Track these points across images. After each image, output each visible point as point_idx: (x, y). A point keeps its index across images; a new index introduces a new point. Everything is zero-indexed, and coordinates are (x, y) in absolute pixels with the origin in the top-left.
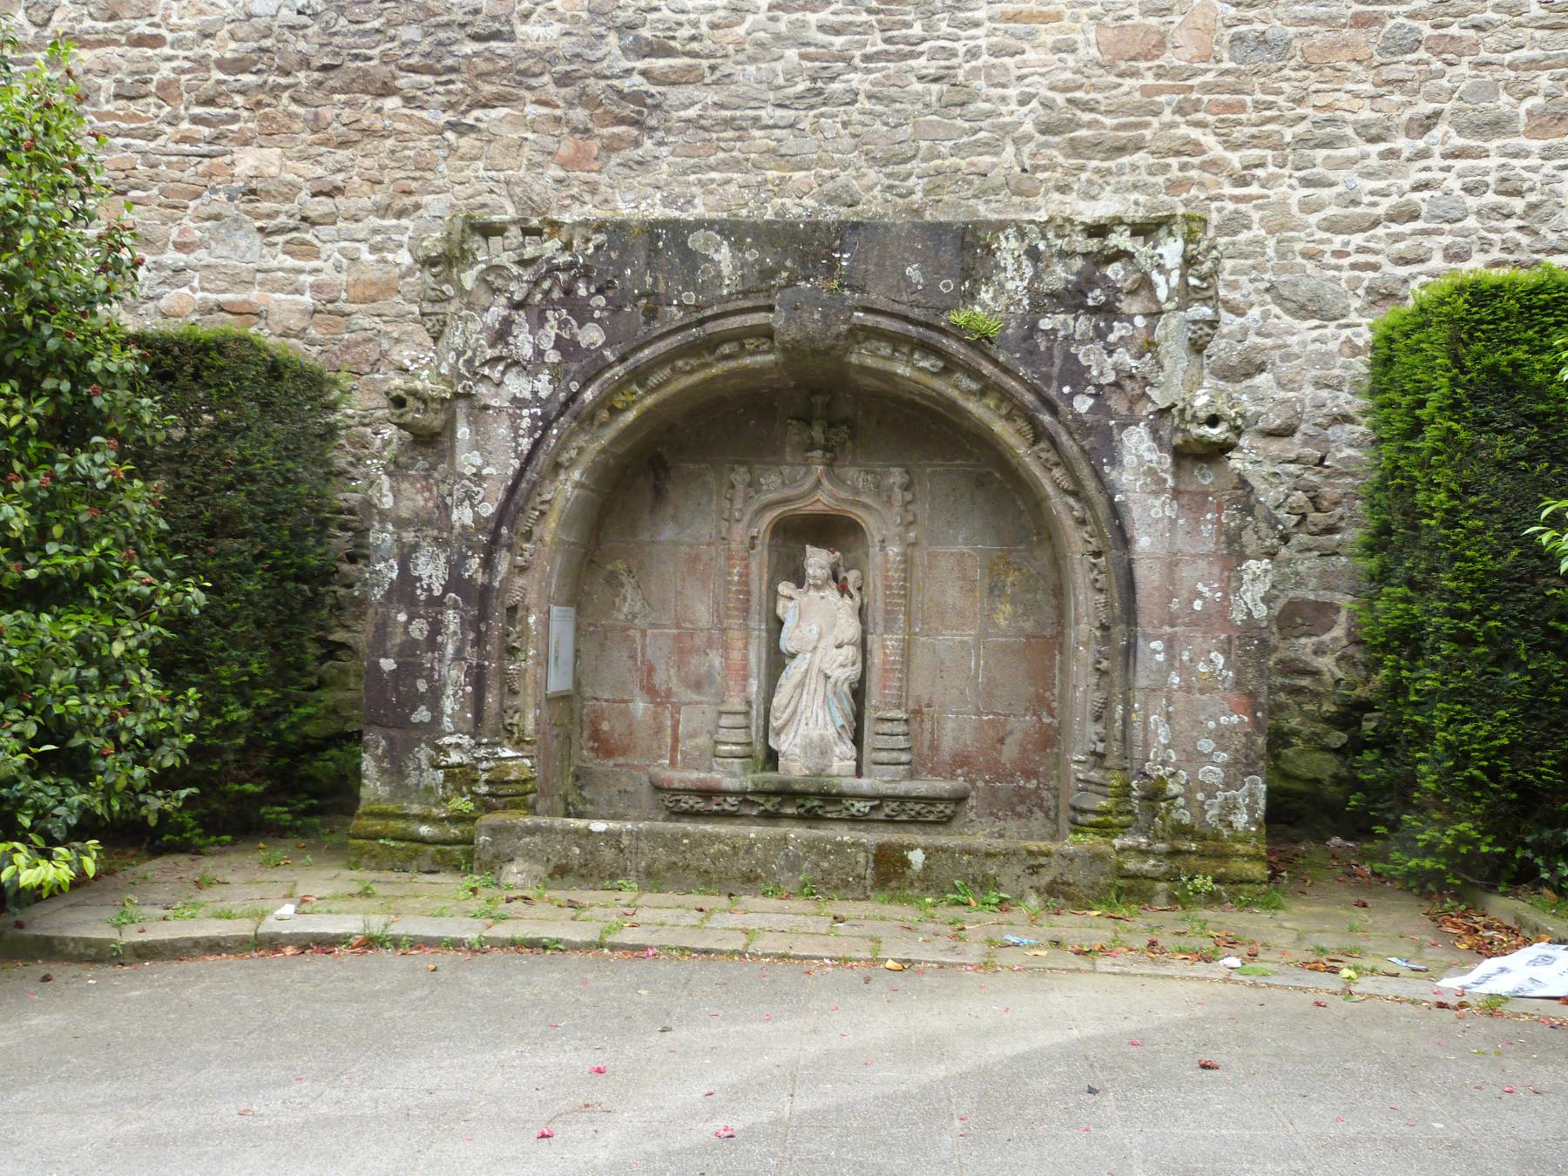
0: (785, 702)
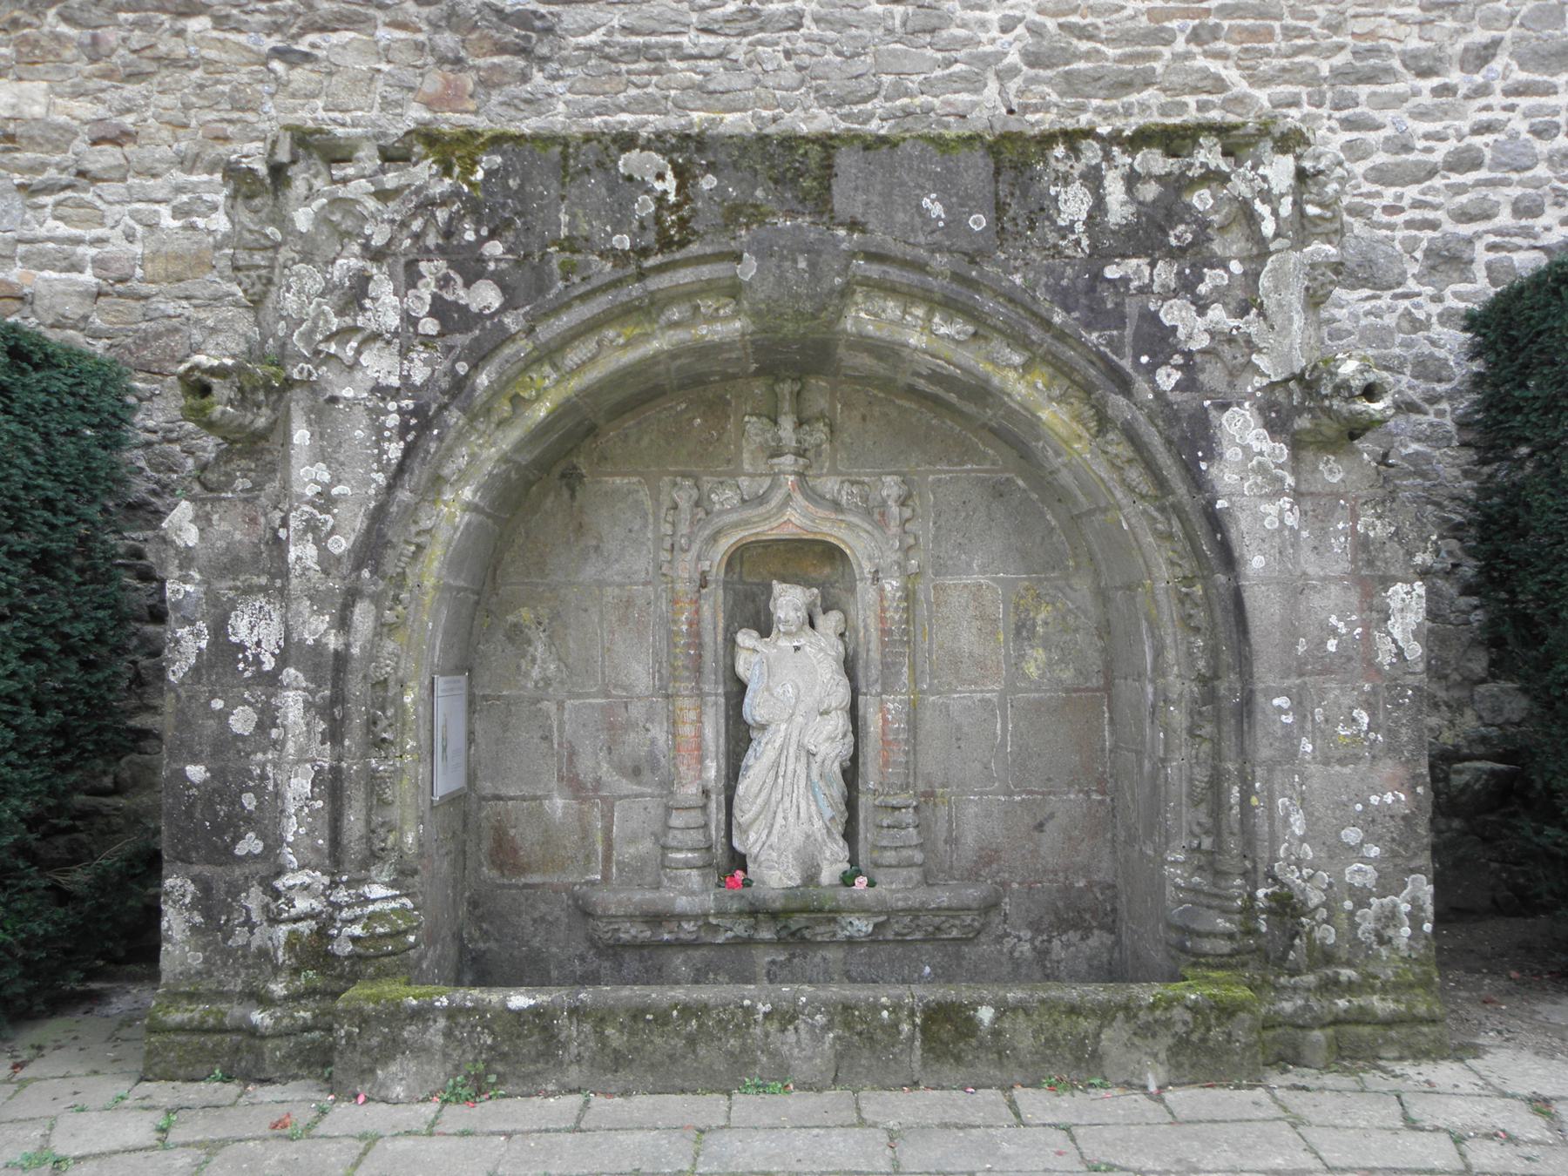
0: (755, 789)
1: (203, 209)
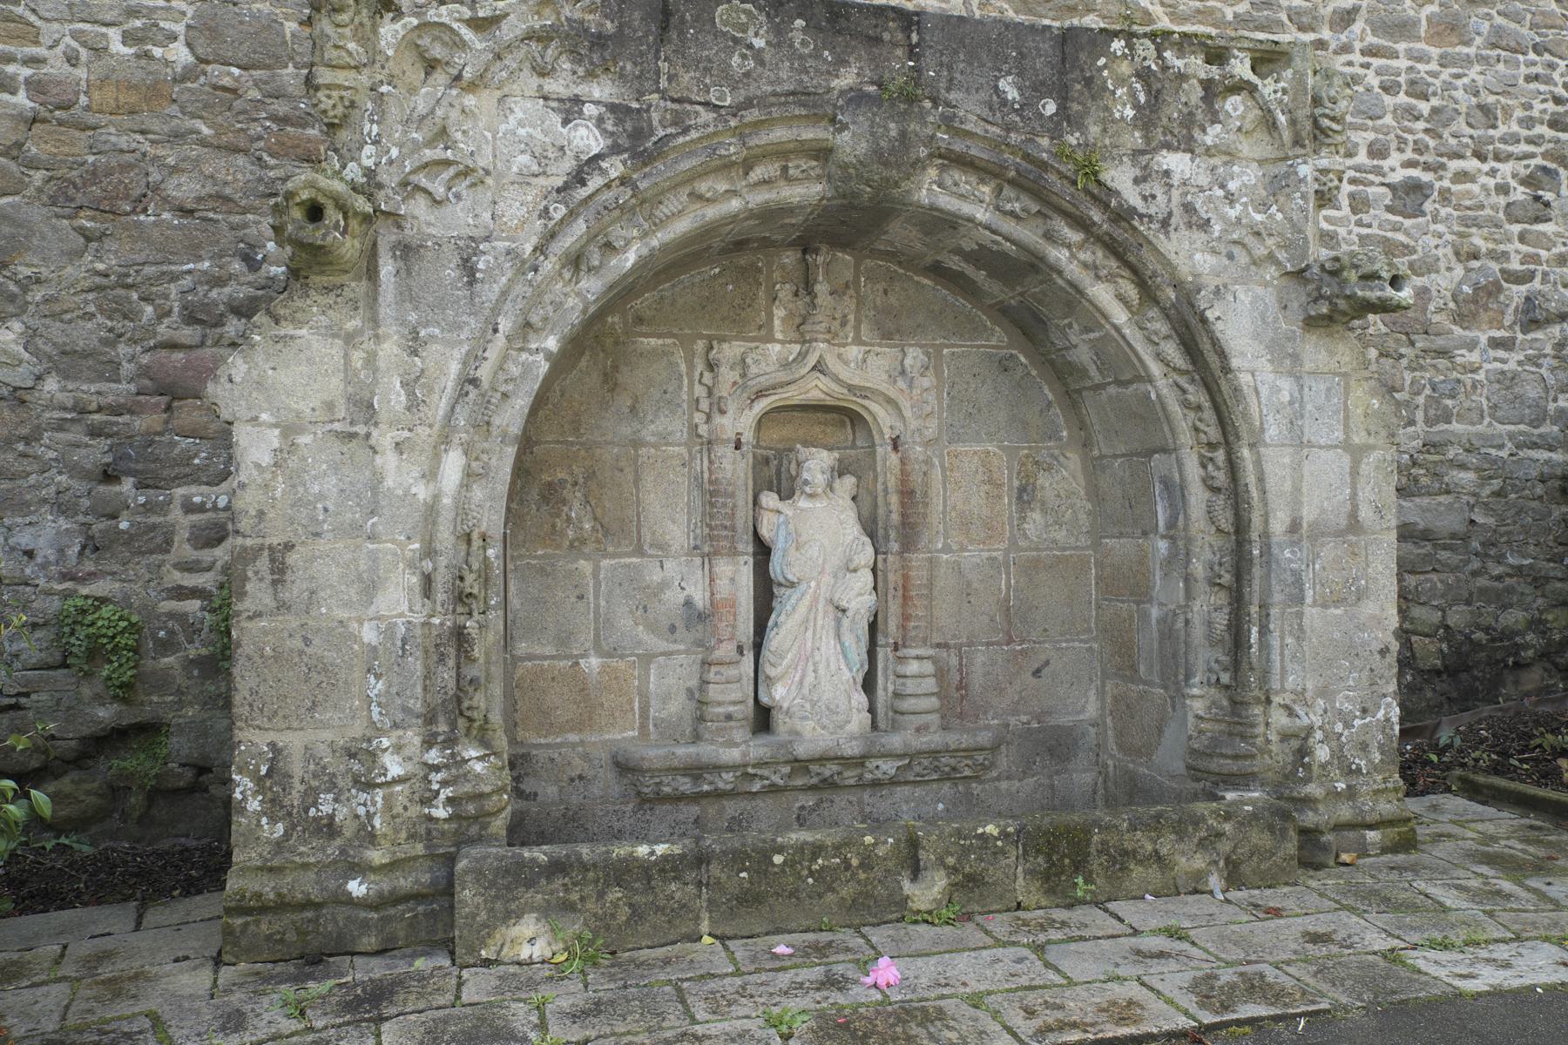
1: (160, 37)
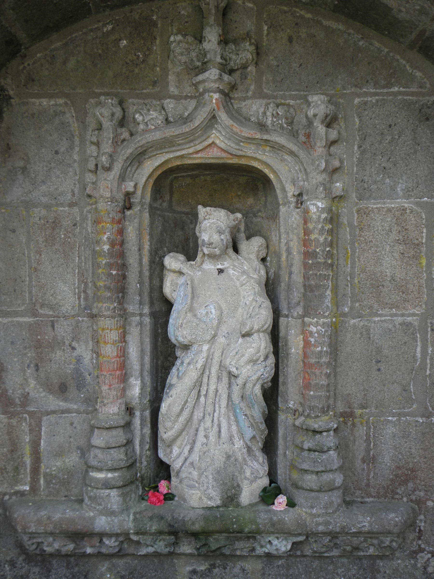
0: (176, 409)
